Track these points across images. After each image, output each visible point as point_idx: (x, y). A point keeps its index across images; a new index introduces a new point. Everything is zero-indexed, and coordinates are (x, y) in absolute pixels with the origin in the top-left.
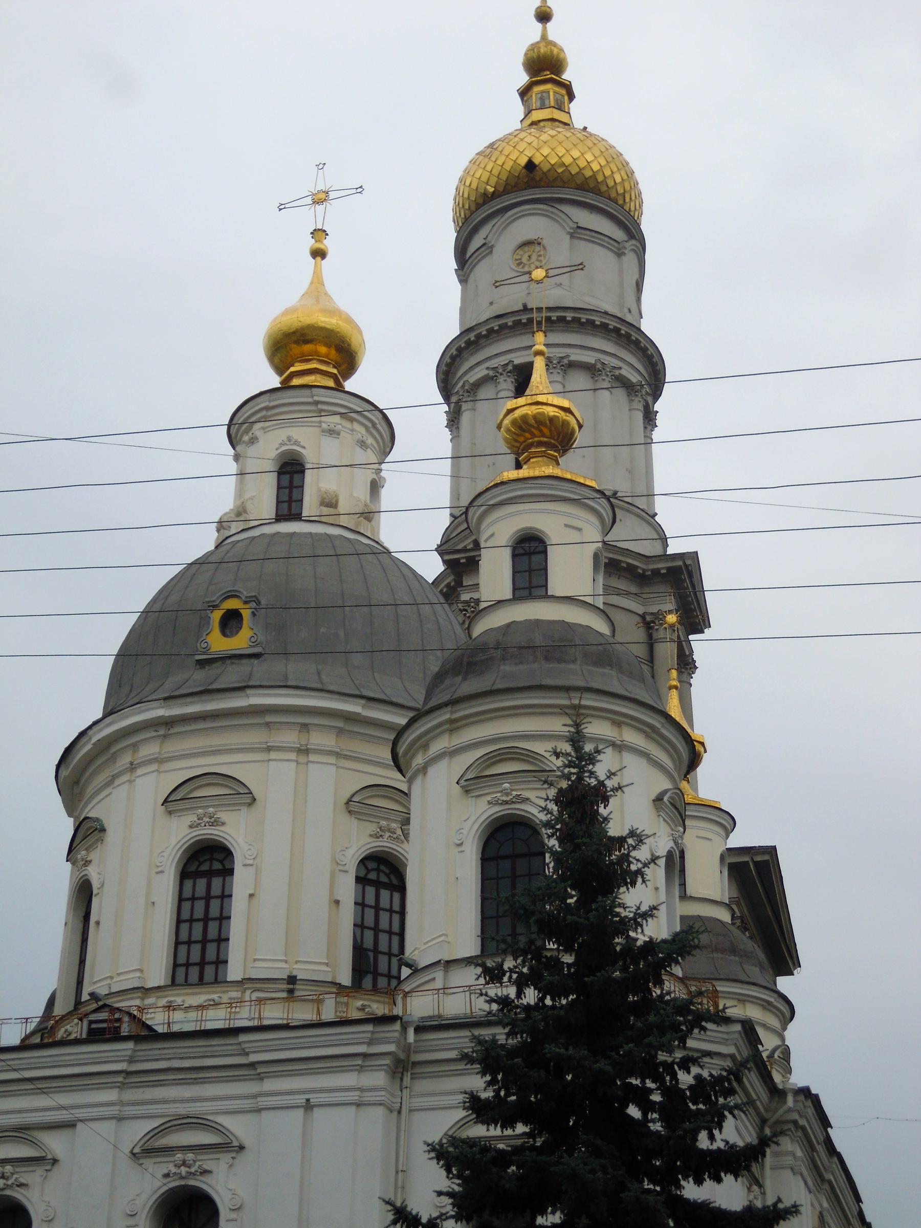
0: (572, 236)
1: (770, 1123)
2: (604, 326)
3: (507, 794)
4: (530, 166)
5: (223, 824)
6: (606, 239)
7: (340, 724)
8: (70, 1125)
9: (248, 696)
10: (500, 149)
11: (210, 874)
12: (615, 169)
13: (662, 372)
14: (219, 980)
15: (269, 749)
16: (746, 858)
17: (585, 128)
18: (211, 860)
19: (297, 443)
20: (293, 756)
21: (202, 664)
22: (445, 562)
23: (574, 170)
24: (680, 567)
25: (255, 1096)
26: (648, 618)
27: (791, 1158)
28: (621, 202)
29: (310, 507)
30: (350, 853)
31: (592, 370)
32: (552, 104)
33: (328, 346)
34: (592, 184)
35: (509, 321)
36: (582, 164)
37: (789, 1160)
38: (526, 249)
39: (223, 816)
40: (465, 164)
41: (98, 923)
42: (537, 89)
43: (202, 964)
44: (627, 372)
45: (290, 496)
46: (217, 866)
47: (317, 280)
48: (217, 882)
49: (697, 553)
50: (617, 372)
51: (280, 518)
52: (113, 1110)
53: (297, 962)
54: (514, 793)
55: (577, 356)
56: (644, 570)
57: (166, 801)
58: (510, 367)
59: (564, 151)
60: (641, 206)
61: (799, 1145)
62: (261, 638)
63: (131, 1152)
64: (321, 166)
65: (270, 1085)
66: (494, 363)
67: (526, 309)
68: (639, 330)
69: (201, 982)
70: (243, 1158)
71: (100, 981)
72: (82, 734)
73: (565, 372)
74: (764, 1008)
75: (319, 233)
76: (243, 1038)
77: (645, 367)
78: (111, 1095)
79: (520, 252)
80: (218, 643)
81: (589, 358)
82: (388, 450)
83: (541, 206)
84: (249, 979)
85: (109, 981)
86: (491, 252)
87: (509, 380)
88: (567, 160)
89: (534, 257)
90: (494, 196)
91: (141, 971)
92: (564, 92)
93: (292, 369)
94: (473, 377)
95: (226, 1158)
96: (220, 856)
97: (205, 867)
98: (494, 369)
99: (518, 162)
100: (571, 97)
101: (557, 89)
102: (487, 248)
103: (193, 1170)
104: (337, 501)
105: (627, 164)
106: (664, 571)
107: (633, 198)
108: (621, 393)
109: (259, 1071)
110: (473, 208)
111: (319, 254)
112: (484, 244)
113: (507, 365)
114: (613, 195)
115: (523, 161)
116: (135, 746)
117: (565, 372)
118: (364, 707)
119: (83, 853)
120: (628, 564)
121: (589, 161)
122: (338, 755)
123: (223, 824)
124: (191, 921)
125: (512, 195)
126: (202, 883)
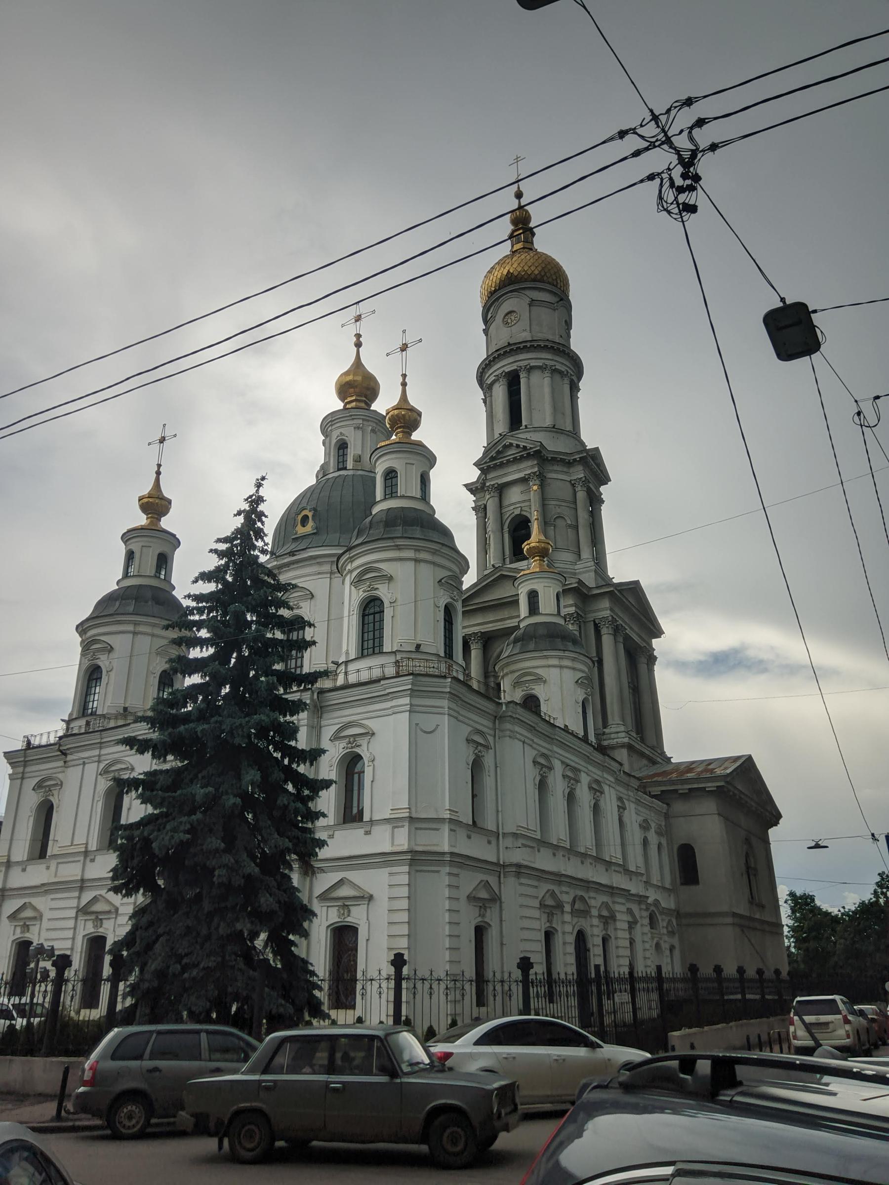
16: (612, 589)
22: (480, 469)
26: (573, 482)
29: (350, 464)
35: (502, 352)
67: (509, 344)
74: (573, 660)
75: (358, 336)
80: (301, 530)
81: (539, 363)
90: (495, 291)
94: (489, 382)
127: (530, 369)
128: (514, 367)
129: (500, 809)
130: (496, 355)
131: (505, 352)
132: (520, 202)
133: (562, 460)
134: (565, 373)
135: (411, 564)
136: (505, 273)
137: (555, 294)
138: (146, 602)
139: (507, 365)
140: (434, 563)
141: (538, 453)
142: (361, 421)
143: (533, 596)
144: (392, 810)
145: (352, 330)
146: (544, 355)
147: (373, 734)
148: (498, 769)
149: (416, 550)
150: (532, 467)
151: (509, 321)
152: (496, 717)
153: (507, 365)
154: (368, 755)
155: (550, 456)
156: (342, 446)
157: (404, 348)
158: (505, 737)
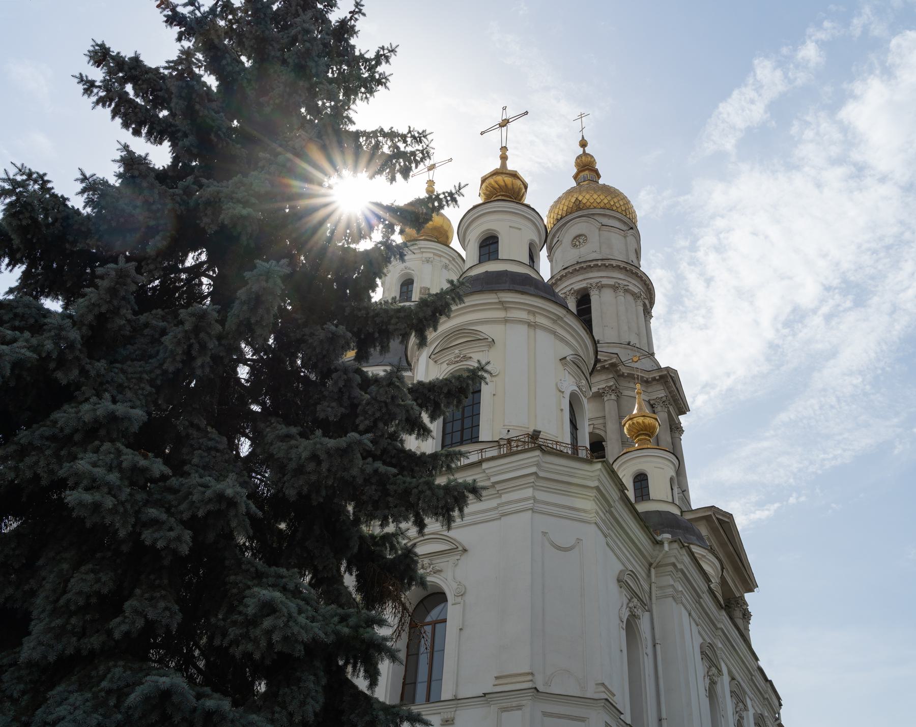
1: (654, 565)
2: (618, 266)
3: (458, 357)
13: (652, 289)
16: (709, 513)
19: (409, 269)
24: (666, 375)
26: (652, 402)
27: (672, 590)
35: (570, 270)
37: (670, 591)
44: (631, 287)
50: (626, 288)
55: (605, 281)
56: (647, 379)
61: (681, 584)
81: (611, 282)
108: (630, 298)
127: (600, 287)
128: (583, 285)
129: (664, 716)
130: (563, 273)
132: (584, 151)
135: (524, 328)
136: (573, 200)
137: (625, 223)
140: (554, 333)
141: (613, 365)
142: (431, 255)
144: (497, 678)
146: (616, 274)
147: (465, 550)
148: (658, 647)
149: (529, 312)
151: (577, 243)
152: (650, 565)
153: (577, 283)
154: (455, 586)
157: (504, 123)
158: (666, 597)
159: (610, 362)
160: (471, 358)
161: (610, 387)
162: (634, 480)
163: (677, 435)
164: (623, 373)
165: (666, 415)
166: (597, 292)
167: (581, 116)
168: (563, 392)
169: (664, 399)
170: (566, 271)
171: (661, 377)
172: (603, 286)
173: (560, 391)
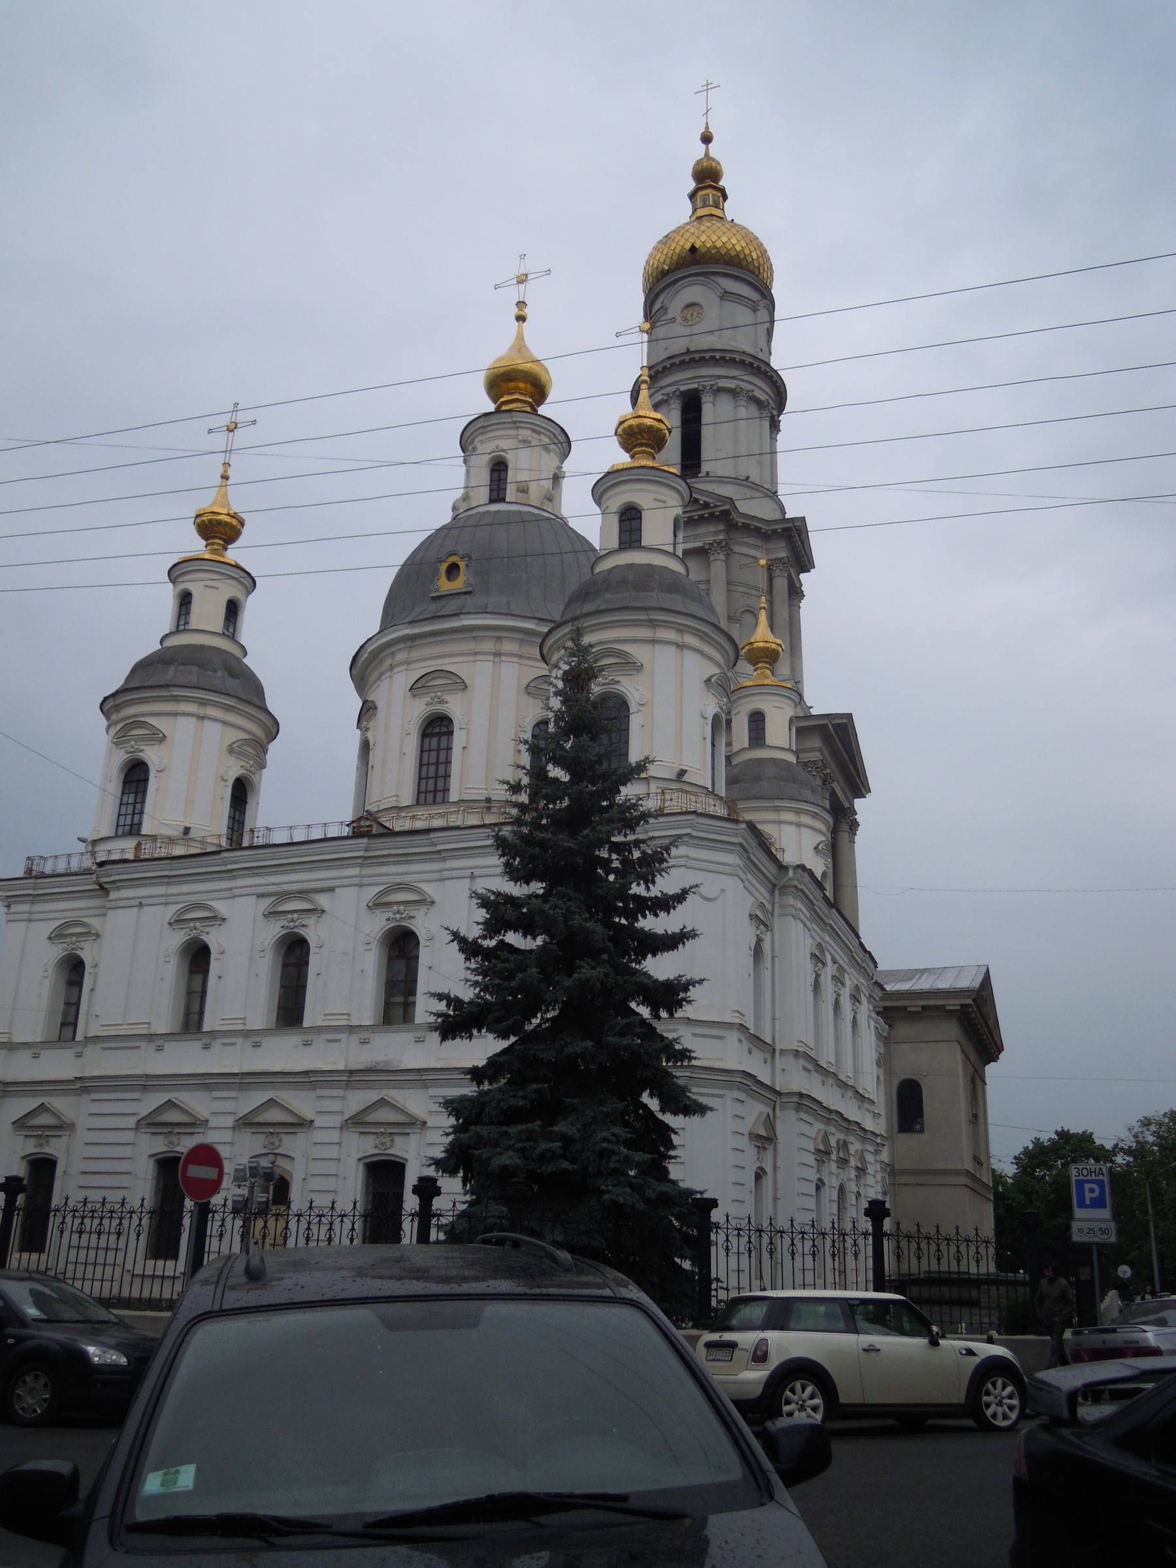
0: (722, 298)
2: (742, 362)
4: (693, 249)
5: (447, 702)
6: (746, 300)
7: (522, 636)
8: (331, 890)
9: (461, 620)
10: (672, 238)
11: (440, 734)
12: (752, 249)
14: (445, 801)
15: (476, 654)
17: (733, 220)
18: (441, 725)
20: (491, 658)
21: (435, 599)
23: (723, 251)
24: (790, 527)
25: (440, 871)
28: (757, 273)
29: (511, 493)
30: (527, 720)
31: (734, 393)
32: (711, 203)
33: (526, 383)
34: (736, 261)
36: (729, 246)
38: (690, 309)
39: (447, 697)
40: (649, 250)
41: (372, 767)
42: (701, 193)
43: (435, 791)
44: (758, 394)
45: (499, 487)
46: (444, 729)
47: (520, 337)
48: (444, 739)
49: (804, 517)
50: (751, 394)
51: (492, 501)
52: (356, 881)
53: (493, 789)
54: (610, 678)
55: (722, 383)
56: (767, 531)
57: (411, 689)
58: (677, 393)
59: (716, 237)
60: (772, 275)
62: (471, 580)
63: (367, 905)
64: (522, 257)
65: (450, 864)
66: (667, 390)
68: (768, 365)
69: (434, 802)
70: (434, 909)
71: (373, 803)
72: (362, 647)
73: (715, 395)
75: (521, 304)
76: (432, 835)
77: (772, 390)
78: (355, 871)
79: (686, 311)
80: (445, 585)
81: (731, 384)
82: (567, 452)
83: (700, 278)
84: (463, 800)
85: (378, 803)
86: (666, 312)
87: (677, 402)
88: (719, 244)
89: (695, 314)
90: (669, 271)
91: (397, 796)
92: (719, 194)
93: (502, 400)
95: (423, 909)
96: (445, 723)
97: (437, 730)
98: (668, 394)
99: (685, 247)
100: (725, 198)
101: (715, 193)
102: (664, 309)
103: (403, 916)
104: (528, 489)
105: (762, 245)
106: (779, 531)
107: (766, 269)
109: (443, 855)
110: (655, 281)
111: (521, 319)
112: (662, 307)
113: (676, 391)
114: (751, 268)
115: (688, 246)
116: (393, 654)
117: (715, 395)
118: (537, 624)
119: (365, 723)
120: (755, 526)
121: (736, 244)
122: (520, 657)
123: (447, 702)
124: (428, 764)
125: (681, 271)
126: (435, 740)
131: (683, 362)
133: (757, 529)
134: (766, 404)
138: (215, 671)
139: (685, 380)
141: (726, 514)
142: (529, 432)
143: (757, 720)
145: (513, 294)
148: (776, 960)
150: (716, 533)
152: (775, 886)
155: (741, 520)
156: (499, 468)
159: (721, 508)
160: (619, 682)
161: (719, 543)
162: (749, 719)
163: (795, 602)
164: (737, 522)
165: (786, 581)
166: (711, 399)
167: (707, 87)
168: (706, 718)
169: (786, 560)
170: (672, 361)
171: (784, 530)
172: (721, 390)
173: (703, 717)
